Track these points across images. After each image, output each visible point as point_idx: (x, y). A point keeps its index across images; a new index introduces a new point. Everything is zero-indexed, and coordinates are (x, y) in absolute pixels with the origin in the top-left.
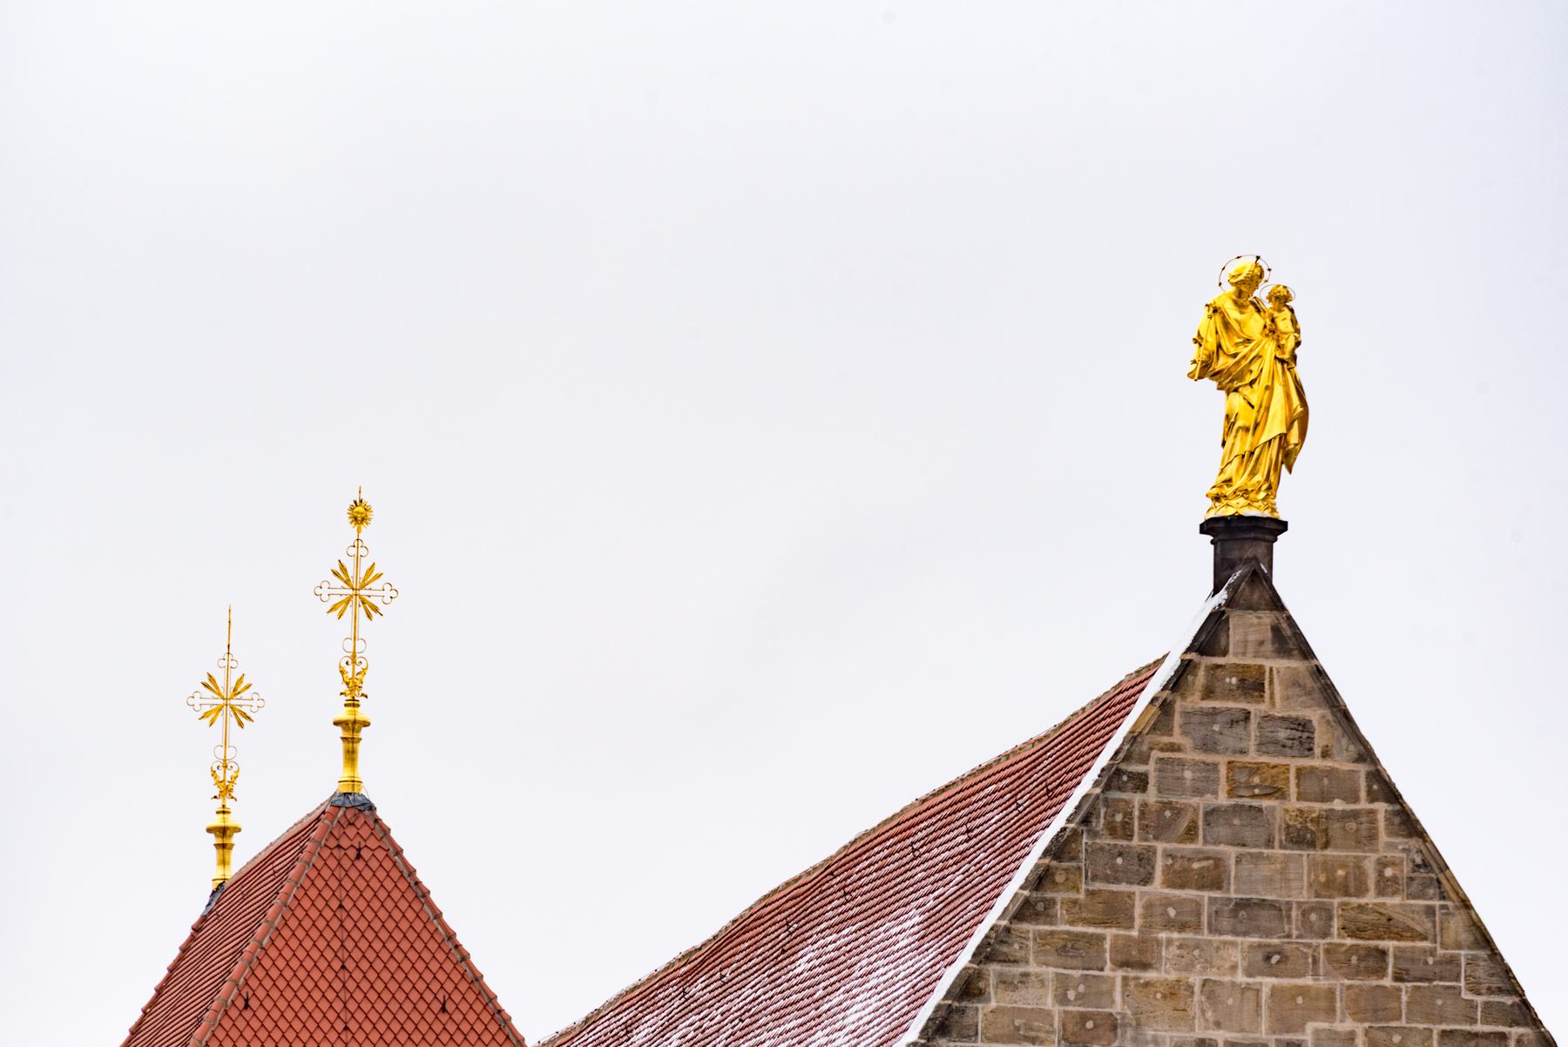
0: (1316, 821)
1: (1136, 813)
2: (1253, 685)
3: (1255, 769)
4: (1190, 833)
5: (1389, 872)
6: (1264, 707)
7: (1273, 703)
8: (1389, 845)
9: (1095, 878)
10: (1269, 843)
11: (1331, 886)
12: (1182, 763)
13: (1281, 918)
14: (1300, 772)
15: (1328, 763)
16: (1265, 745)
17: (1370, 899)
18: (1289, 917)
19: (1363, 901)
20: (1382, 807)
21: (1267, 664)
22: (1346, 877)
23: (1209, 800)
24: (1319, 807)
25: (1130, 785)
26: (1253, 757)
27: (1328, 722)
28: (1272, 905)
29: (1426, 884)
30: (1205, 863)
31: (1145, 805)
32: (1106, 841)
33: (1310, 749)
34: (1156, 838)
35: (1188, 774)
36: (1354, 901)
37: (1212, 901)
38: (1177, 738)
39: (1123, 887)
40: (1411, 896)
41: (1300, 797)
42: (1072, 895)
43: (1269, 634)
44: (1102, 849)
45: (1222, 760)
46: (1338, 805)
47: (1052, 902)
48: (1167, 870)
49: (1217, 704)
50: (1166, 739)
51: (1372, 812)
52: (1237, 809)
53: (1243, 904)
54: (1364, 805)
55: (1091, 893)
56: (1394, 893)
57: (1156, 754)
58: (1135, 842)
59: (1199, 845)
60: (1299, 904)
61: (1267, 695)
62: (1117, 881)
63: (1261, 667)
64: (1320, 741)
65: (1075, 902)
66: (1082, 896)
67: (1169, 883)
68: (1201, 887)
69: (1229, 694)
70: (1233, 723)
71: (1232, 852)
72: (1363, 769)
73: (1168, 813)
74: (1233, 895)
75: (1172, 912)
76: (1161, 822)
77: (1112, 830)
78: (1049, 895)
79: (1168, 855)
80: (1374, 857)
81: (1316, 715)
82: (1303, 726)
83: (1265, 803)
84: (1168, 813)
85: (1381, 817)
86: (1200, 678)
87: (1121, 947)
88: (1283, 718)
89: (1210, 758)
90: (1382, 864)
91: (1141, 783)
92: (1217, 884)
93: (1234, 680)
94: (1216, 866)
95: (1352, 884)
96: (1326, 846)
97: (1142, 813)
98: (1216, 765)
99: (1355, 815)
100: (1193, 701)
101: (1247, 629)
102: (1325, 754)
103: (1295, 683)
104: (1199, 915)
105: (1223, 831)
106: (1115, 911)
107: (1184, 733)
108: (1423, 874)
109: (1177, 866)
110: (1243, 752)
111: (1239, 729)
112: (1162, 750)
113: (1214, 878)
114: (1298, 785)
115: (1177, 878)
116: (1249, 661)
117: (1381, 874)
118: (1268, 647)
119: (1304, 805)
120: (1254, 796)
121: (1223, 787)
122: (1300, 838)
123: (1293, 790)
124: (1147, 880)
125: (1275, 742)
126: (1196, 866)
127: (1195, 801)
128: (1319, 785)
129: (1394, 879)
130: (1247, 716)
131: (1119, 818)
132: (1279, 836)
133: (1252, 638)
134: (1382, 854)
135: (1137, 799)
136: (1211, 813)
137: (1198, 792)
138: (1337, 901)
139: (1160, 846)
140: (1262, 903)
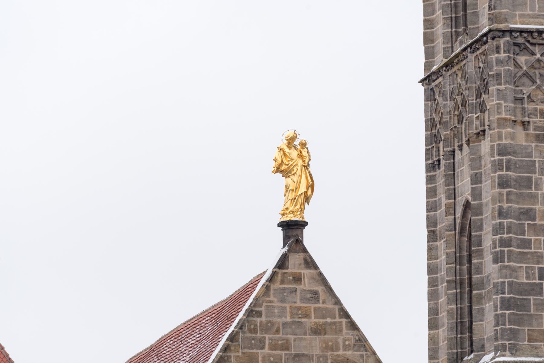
0: (321, 326)
1: (258, 325)
2: (297, 279)
3: (299, 308)
4: (277, 331)
5: (347, 343)
6: (302, 287)
7: (305, 285)
8: (347, 334)
9: (245, 348)
10: (305, 334)
11: (327, 348)
12: (274, 307)
13: (310, 360)
14: (315, 309)
15: (325, 306)
16: (303, 299)
17: (341, 352)
18: (313, 359)
19: (338, 353)
20: (344, 320)
21: (302, 272)
22: (332, 345)
23: (284, 320)
24: (322, 321)
25: (256, 315)
26: (299, 304)
27: (324, 291)
28: (307, 355)
29: (360, 347)
30: (283, 342)
31: (261, 322)
32: (248, 335)
33: (318, 301)
34: (266, 333)
35: (276, 311)
36: (335, 353)
37: (286, 354)
38: (272, 298)
39: (255, 351)
40: (355, 351)
41: (315, 318)
42: (237, 354)
43: (303, 261)
44: (247, 338)
45: (287, 305)
46: (329, 320)
47: (230, 357)
48: (270, 344)
49: (286, 286)
50: (268, 299)
51: (341, 322)
52: (294, 323)
53: (297, 355)
54: (337, 320)
55: (243, 353)
56: (349, 350)
57: (264, 304)
58: (258, 335)
59: (280, 335)
60: (316, 355)
61: (303, 282)
62: (253, 349)
63: (300, 273)
64: (322, 297)
65: (238, 356)
66: (240, 354)
67: (271, 349)
68: (282, 350)
69: (290, 282)
70: (291, 292)
71: (292, 337)
72: (337, 307)
73: (269, 325)
74: (293, 352)
75: (272, 359)
76: (267, 328)
77: (250, 331)
78: (229, 354)
79: (270, 339)
80: (342, 337)
81: (320, 289)
82: (315, 293)
83: (303, 320)
84: (269, 325)
85: (344, 324)
86: (279, 277)
88: (309, 291)
89: (284, 305)
90: (345, 340)
91: (259, 314)
92: (287, 349)
93: (291, 278)
94: (287, 343)
95: (334, 347)
96: (325, 334)
97: (261, 325)
98: (285, 308)
99: (334, 323)
100: (277, 285)
101: (295, 260)
102: (324, 302)
103: (313, 278)
104: (281, 360)
105: (289, 330)
107: (274, 297)
108: (359, 343)
109: (273, 343)
110: (295, 302)
111: (293, 295)
112: (267, 302)
113: (286, 347)
114: (314, 314)
115: (273, 347)
116: (296, 271)
117: (344, 343)
118: (303, 266)
119: (317, 320)
120: (299, 318)
121: (288, 315)
122: (317, 331)
123: (313, 315)
124: (263, 348)
125: (306, 299)
126: (280, 342)
127: (279, 320)
128: (322, 313)
129: (349, 345)
130: (296, 290)
131: (252, 327)
132: (308, 332)
133: (297, 263)
134: (344, 336)
135: (258, 320)
136: (285, 324)
137: (280, 317)
138: (329, 353)
139: (267, 336)
140: (303, 355)
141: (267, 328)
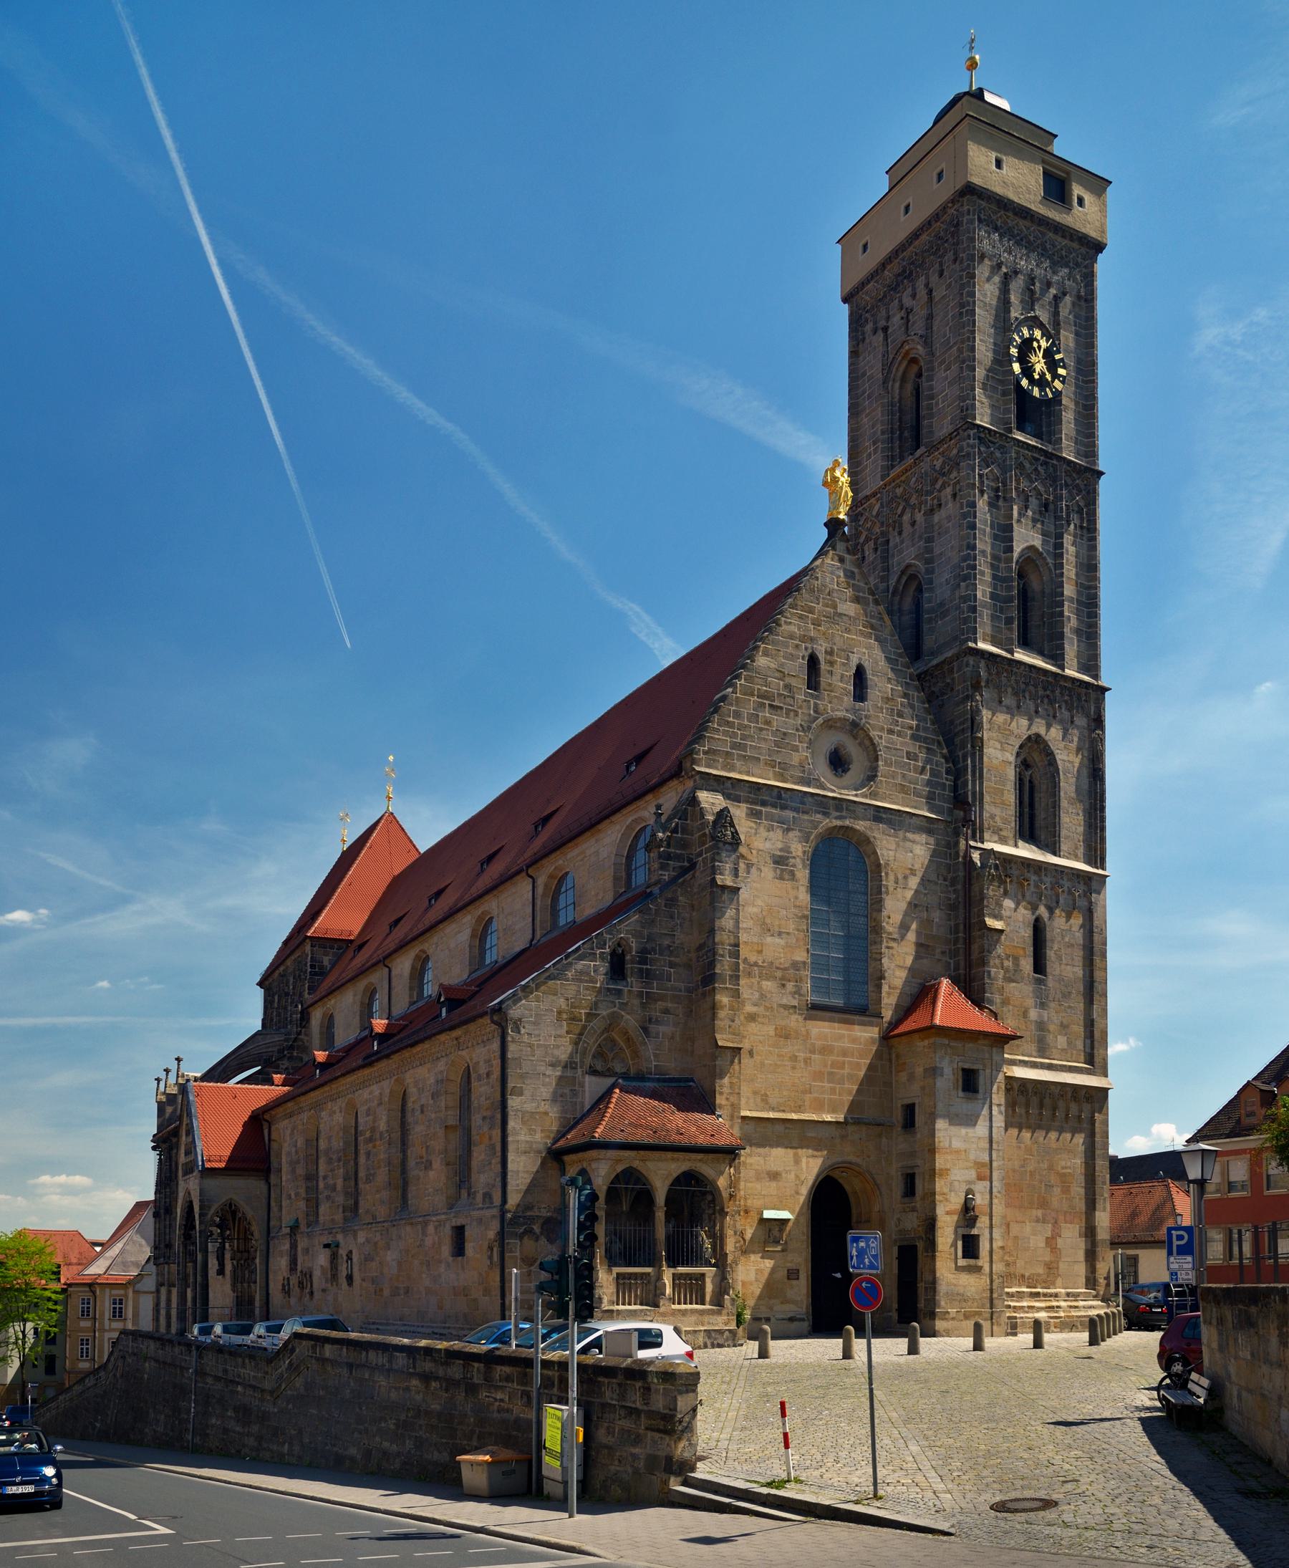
82: (853, 573)
87: (813, 619)
106: (811, 611)
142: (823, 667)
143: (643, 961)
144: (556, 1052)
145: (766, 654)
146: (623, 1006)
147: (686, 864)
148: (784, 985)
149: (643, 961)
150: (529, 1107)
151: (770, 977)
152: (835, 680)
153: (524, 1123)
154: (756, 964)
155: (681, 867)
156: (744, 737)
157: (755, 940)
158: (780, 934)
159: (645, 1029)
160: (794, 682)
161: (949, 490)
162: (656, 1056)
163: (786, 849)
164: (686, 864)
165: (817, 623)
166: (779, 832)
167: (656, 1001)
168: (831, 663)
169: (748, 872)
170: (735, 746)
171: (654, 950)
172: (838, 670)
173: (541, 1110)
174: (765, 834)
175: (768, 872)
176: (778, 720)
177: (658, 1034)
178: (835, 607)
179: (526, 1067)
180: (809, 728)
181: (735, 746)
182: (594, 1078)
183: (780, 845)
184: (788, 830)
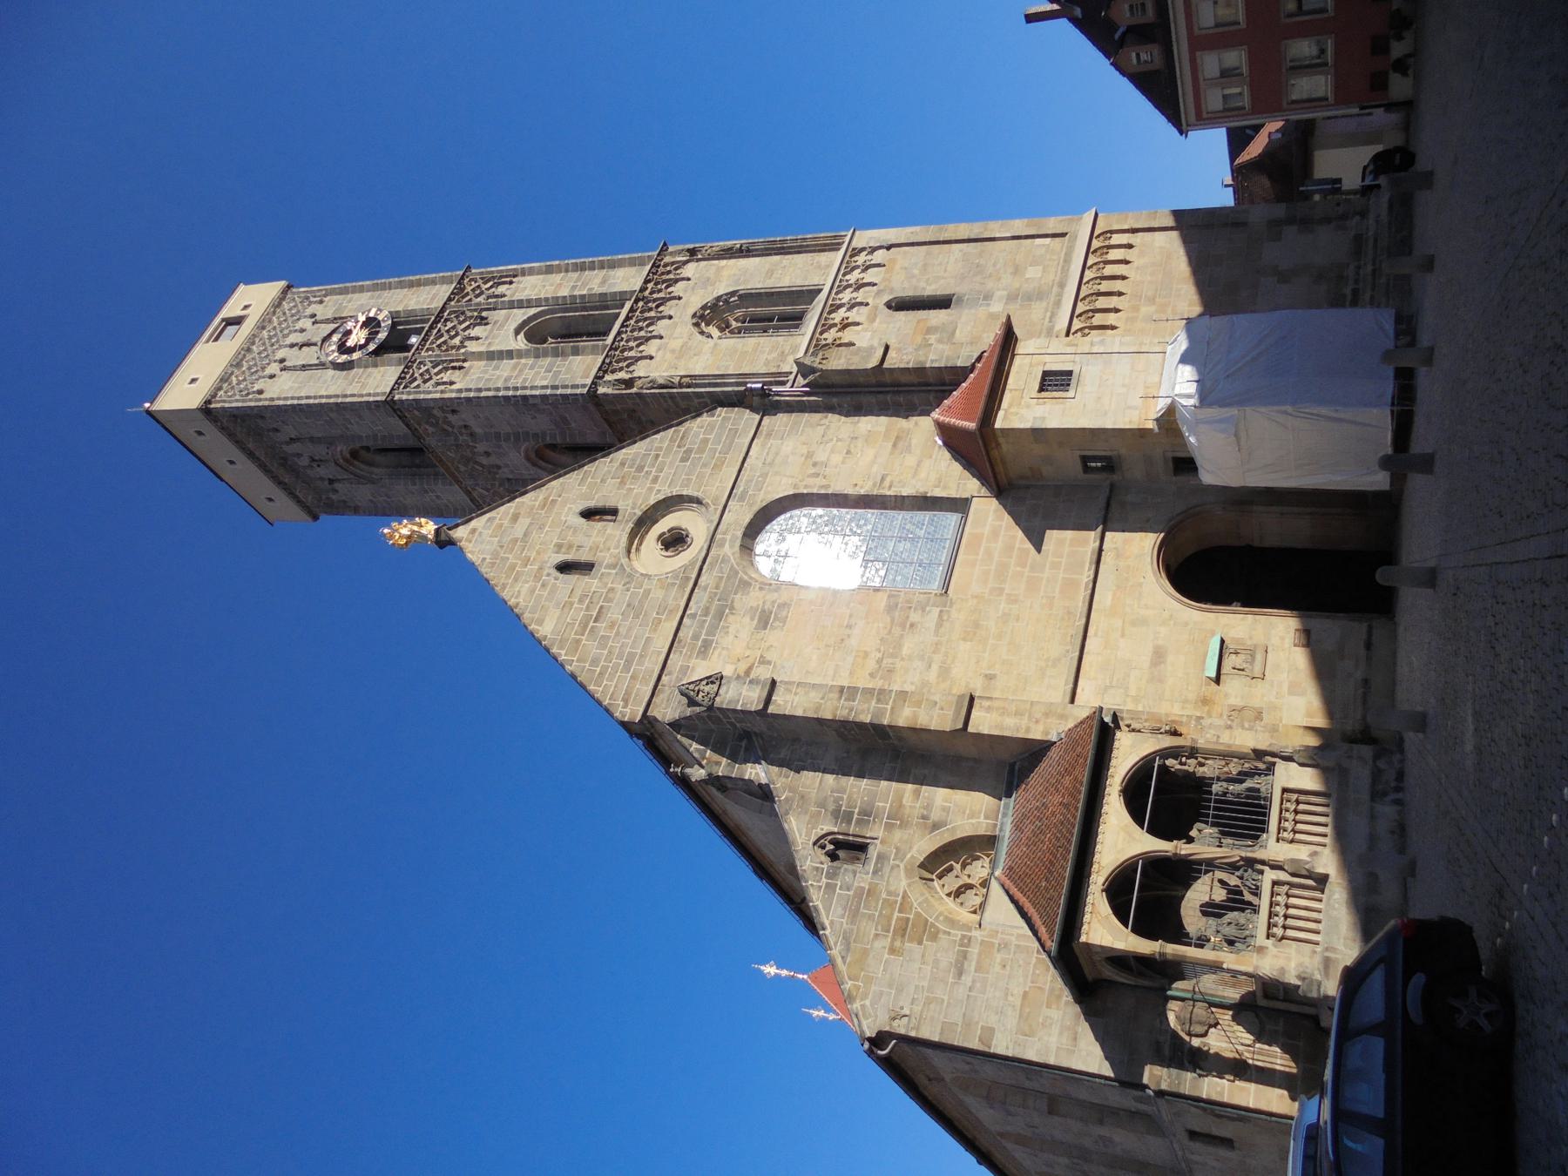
106: (513, 567)
141: (495, 555)
142: (569, 557)
143: (848, 817)
144: (943, 964)
145: (540, 622)
146: (900, 853)
147: (744, 744)
148: (912, 625)
149: (848, 817)
150: (1011, 1021)
151: (899, 646)
152: (588, 543)
153: (1031, 1034)
154: (879, 661)
155: (747, 749)
156: (620, 656)
157: (850, 659)
158: (849, 627)
159: (936, 826)
160: (578, 593)
161: (451, 418)
162: (972, 816)
163: (753, 610)
164: (744, 744)
165: (526, 561)
166: (731, 619)
167: (901, 806)
168: (570, 546)
169: (769, 663)
170: (627, 668)
171: (836, 801)
172: (579, 539)
173: (1018, 1003)
174: (731, 637)
175: (773, 637)
176: (614, 614)
177: (946, 810)
178: (516, 540)
179: (956, 1017)
180: (630, 575)
181: (627, 668)
182: (987, 914)
183: (747, 619)
184: (732, 608)
